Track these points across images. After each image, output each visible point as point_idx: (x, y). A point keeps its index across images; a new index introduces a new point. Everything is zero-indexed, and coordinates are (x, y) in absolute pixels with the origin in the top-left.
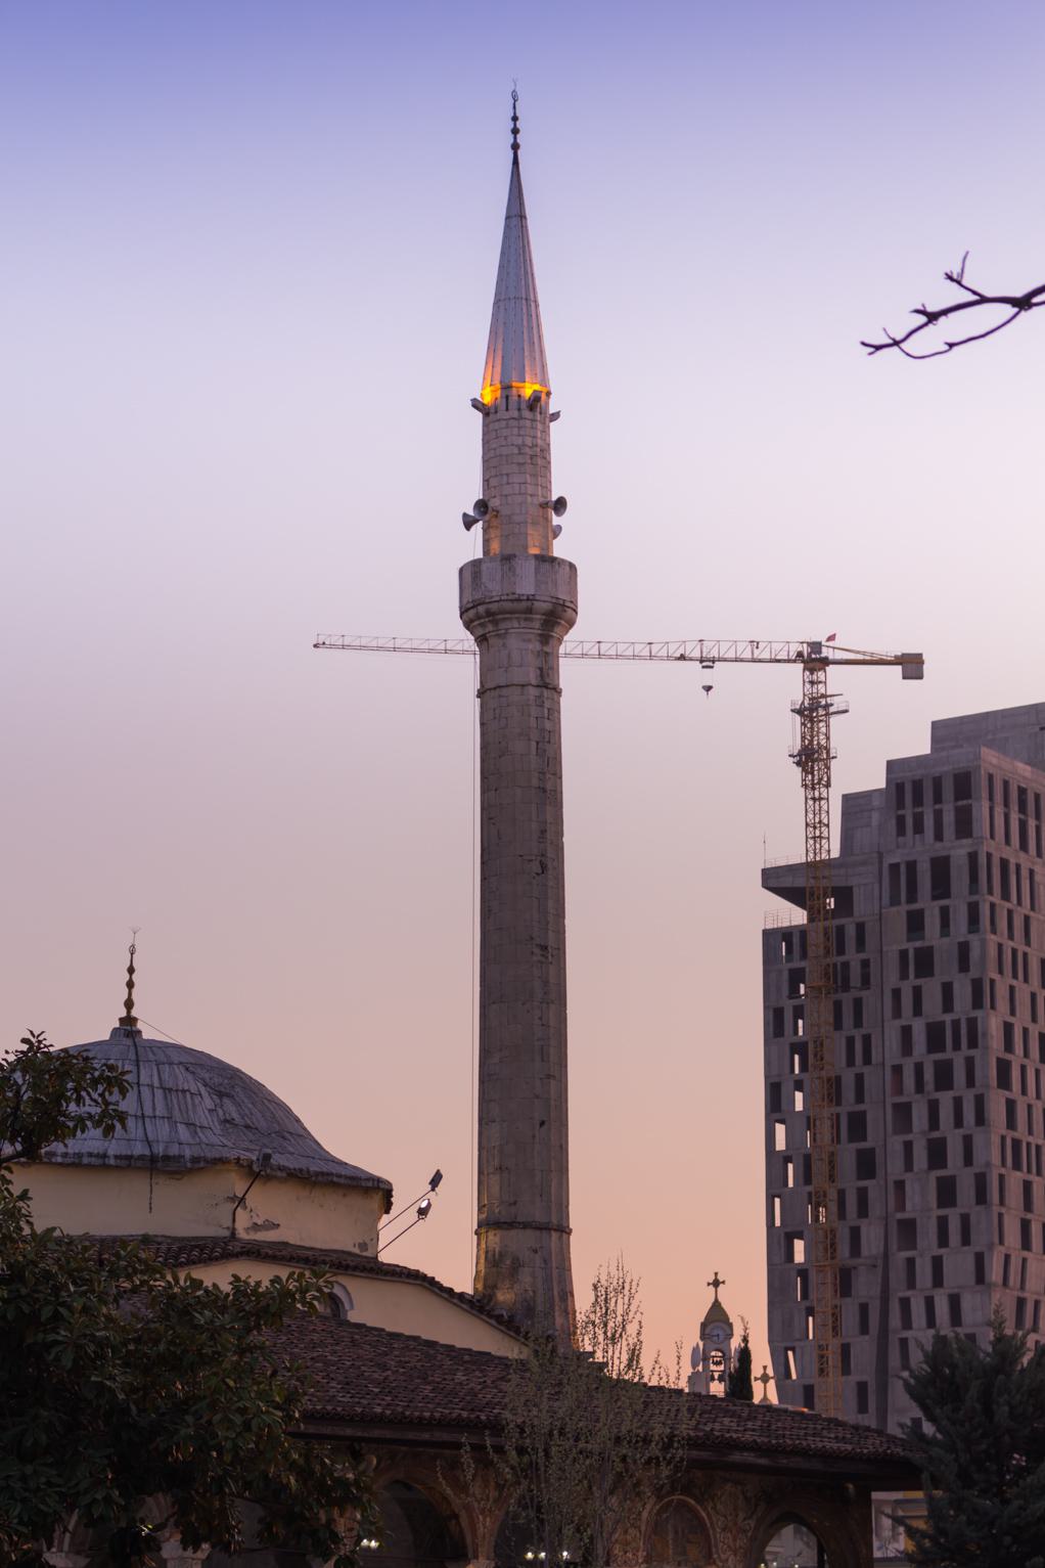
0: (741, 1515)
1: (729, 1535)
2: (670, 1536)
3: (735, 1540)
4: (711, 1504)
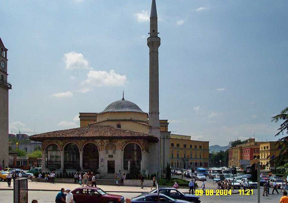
2: (110, 147)
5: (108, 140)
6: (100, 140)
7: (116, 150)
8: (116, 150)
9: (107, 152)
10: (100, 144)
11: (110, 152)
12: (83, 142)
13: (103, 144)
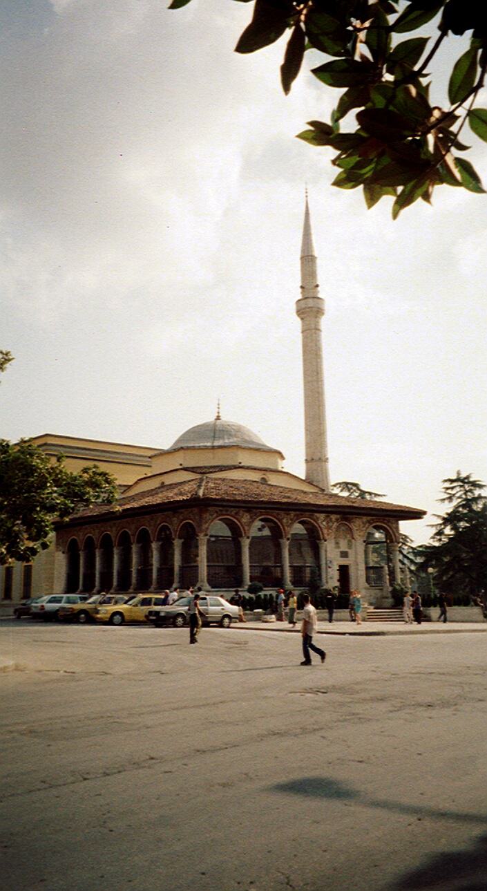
10: (324, 523)
12: (292, 517)
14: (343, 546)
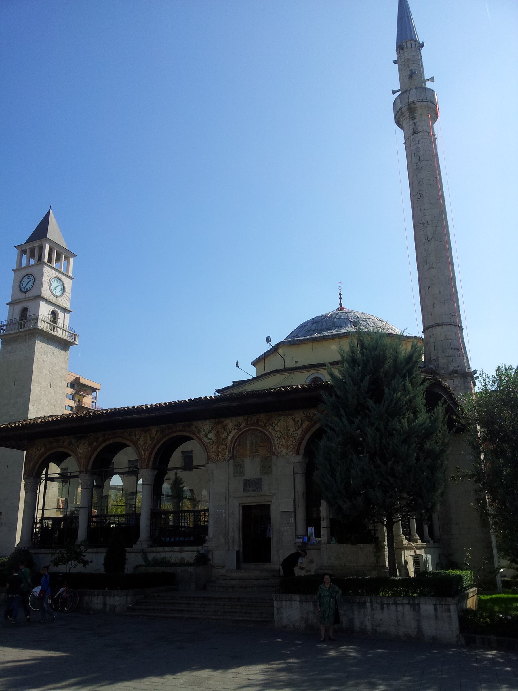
0: (291, 430)
1: (283, 440)
2: (249, 445)
3: (287, 441)
4: (271, 427)
5: (241, 419)
6: (214, 420)
7: (274, 458)
8: (274, 458)
9: (239, 469)
10: (211, 435)
11: (251, 469)
13: (225, 434)
14: (251, 469)
